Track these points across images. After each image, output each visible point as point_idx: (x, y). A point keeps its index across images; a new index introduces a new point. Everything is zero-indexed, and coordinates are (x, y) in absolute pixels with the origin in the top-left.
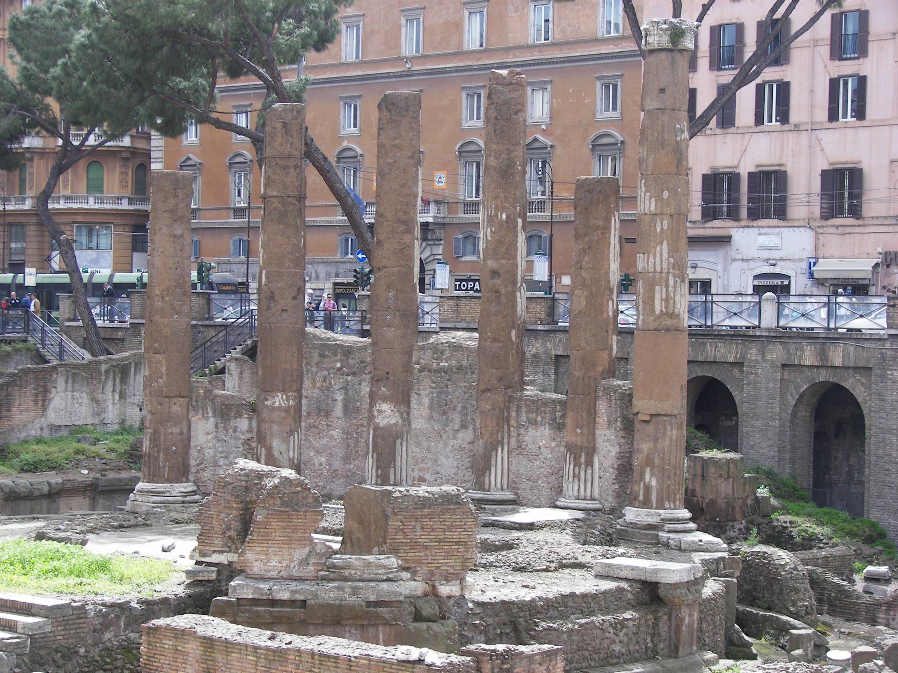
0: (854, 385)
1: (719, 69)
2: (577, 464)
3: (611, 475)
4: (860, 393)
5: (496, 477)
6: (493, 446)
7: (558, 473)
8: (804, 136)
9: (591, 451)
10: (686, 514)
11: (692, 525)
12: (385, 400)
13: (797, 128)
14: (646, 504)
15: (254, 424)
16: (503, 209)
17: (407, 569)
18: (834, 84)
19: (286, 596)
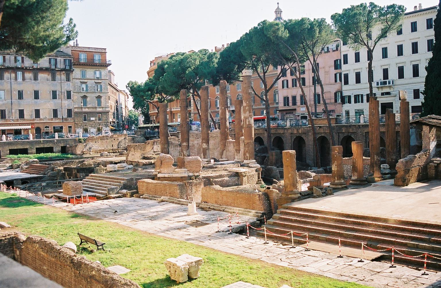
0: (303, 136)
1: (292, 76)
2: (237, 153)
3: (243, 155)
4: (304, 138)
5: (224, 156)
6: (223, 151)
7: (234, 154)
8: (308, 88)
9: (239, 150)
10: (255, 161)
11: (256, 163)
12: (204, 143)
13: (307, 87)
14: (247, 159)
15: (181, 149)
16: (223, 107)
17: (189, 171)
18: (336, 75)
19: (167, 176)
